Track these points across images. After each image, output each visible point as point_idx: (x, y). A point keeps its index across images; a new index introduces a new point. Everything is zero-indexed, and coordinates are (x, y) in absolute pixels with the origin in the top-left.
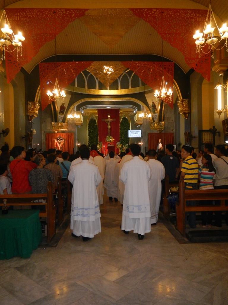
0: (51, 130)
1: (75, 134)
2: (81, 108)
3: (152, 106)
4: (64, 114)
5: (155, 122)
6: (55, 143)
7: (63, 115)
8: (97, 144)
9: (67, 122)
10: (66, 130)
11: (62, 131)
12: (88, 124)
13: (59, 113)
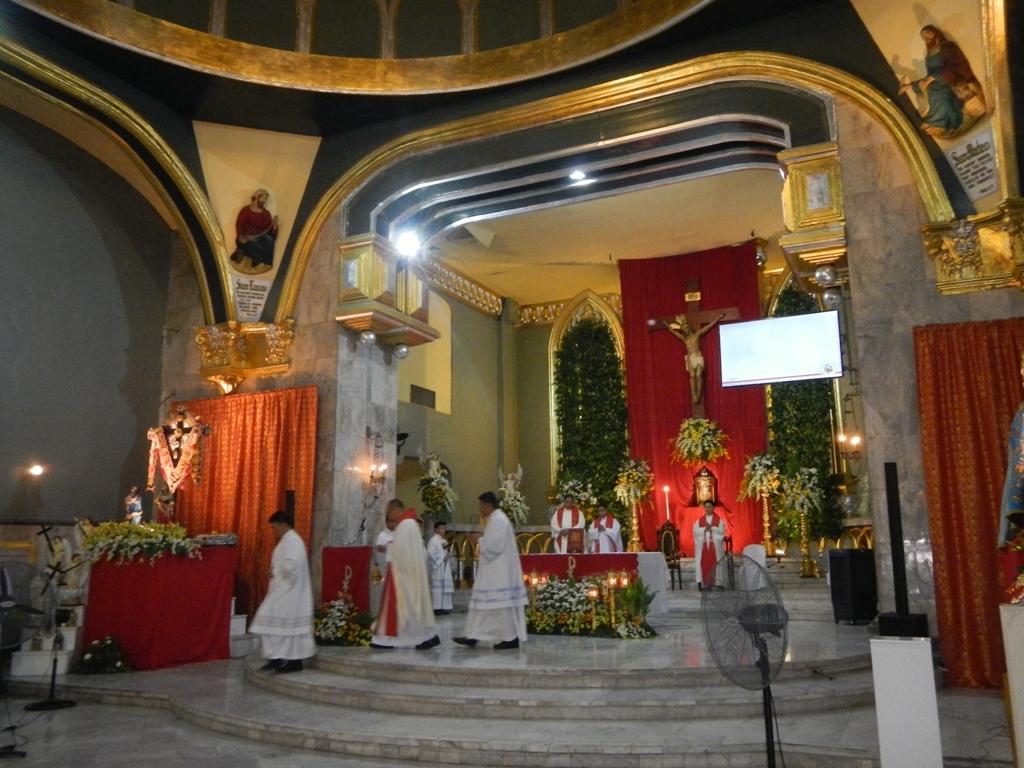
0: (204, 383)
1: (335, 396)
2: (373, 214)
3: (931, 71)
4: (269, 261)
5: (975, 213)
6: (151, 461)
7: (273, 273)
8: (617, 478)
9: (287, 318)
10: (283, 368)
11: (259, 380)
12: (558, 355)
13: (235, 258)
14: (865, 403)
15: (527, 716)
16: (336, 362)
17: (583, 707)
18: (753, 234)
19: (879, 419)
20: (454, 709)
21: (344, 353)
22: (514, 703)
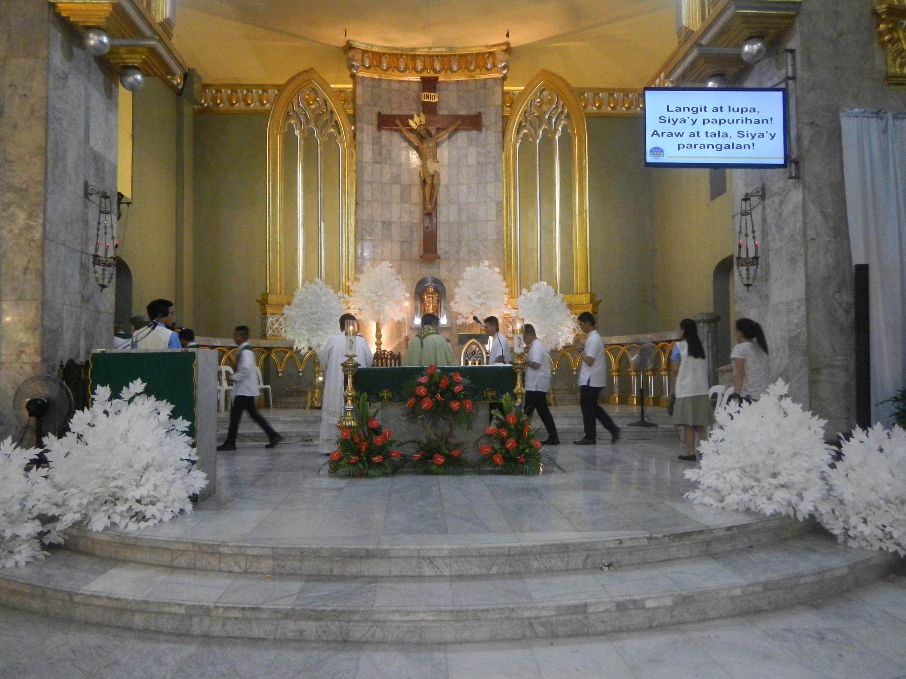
14: (808, 199)
15: (655, 624)
16: (48, 67)
17: (732, 598)
18: (508, 36)
19: (819, 219)
20: (531, 624)
21: (57, 57)
22: (637, 604)
